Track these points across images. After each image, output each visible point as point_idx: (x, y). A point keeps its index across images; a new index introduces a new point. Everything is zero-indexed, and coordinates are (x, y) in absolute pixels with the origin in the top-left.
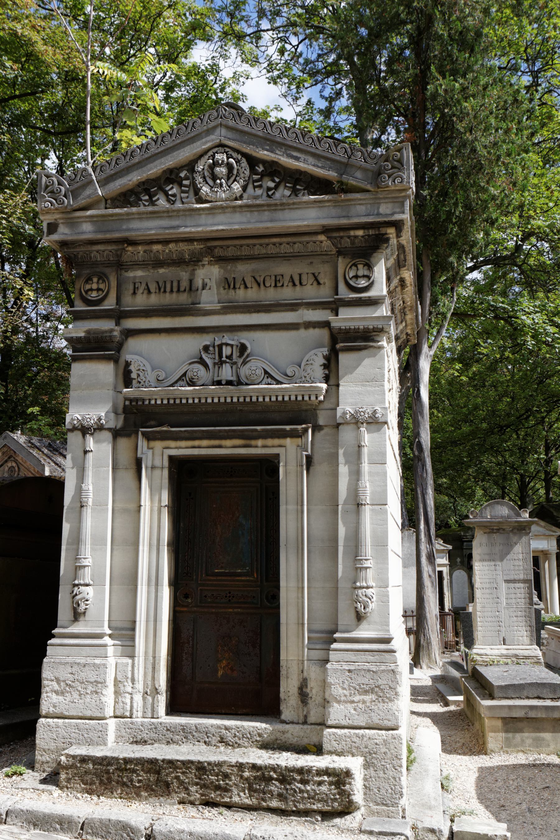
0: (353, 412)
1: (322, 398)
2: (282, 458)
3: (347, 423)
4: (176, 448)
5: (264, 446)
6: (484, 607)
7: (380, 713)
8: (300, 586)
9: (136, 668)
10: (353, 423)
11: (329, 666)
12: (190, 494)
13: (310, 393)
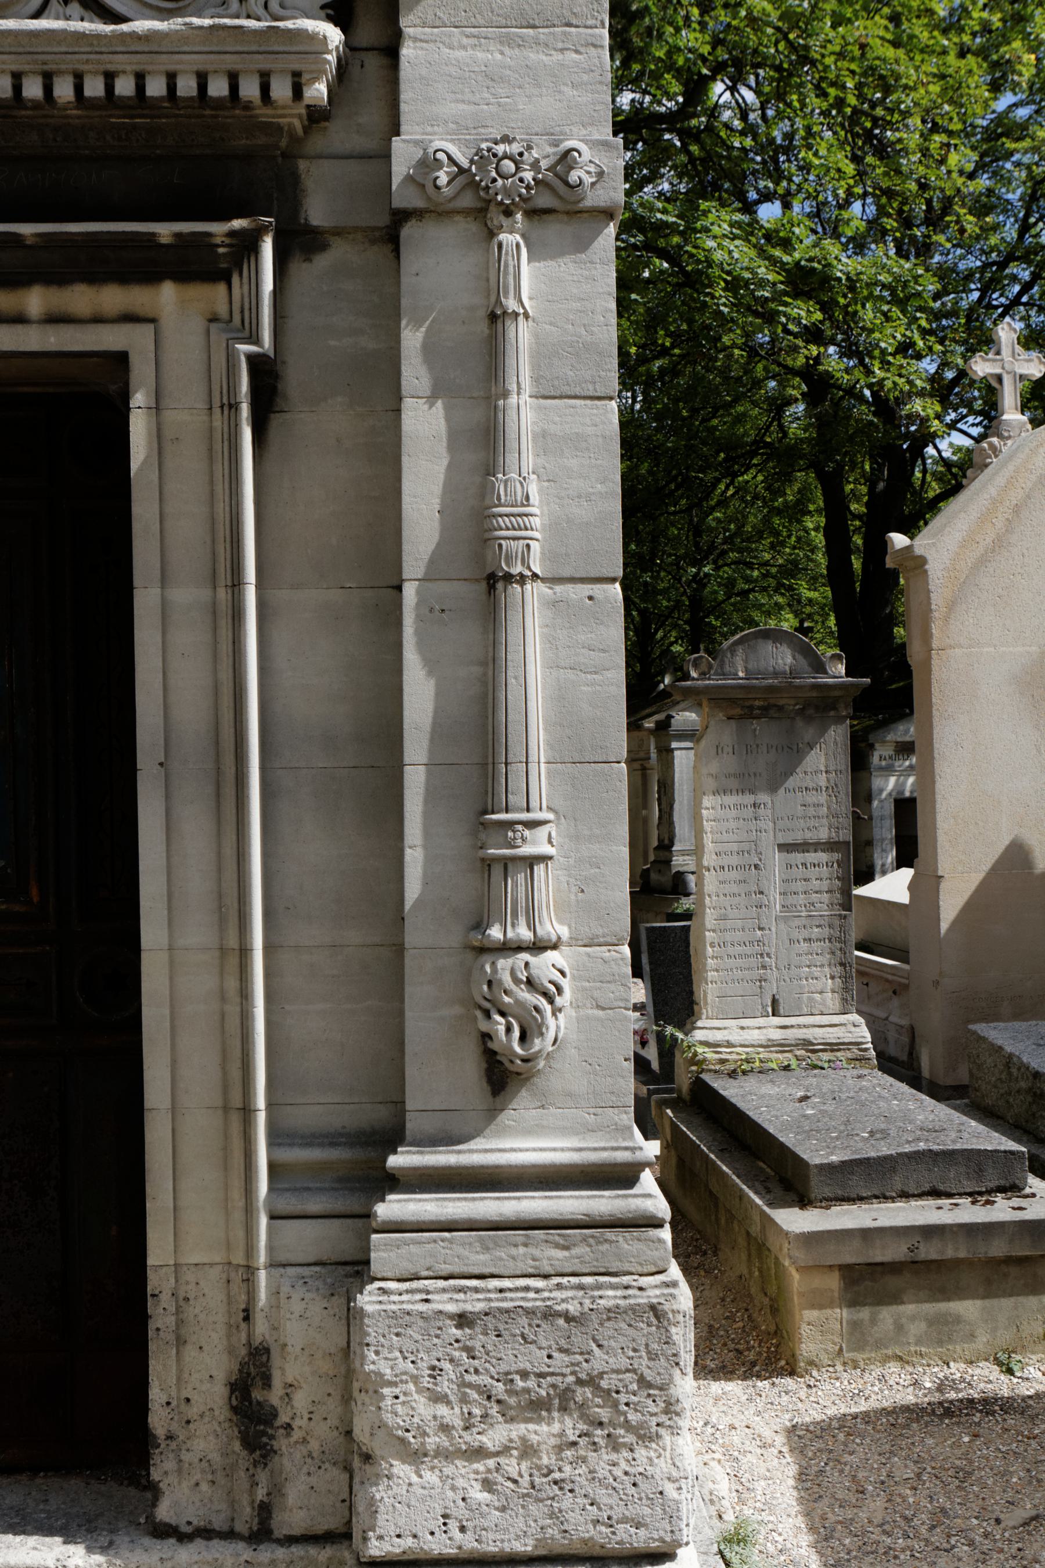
0: (465, 163)
1: (319, 90)
2: (141, 370)
3: (436, 212)
5: (55, 319)
6: (724, 918)
7: (602, 1495)
8: (233, 942)
10: (465, 212)
11: (368, 1300)
13: (263, 63)
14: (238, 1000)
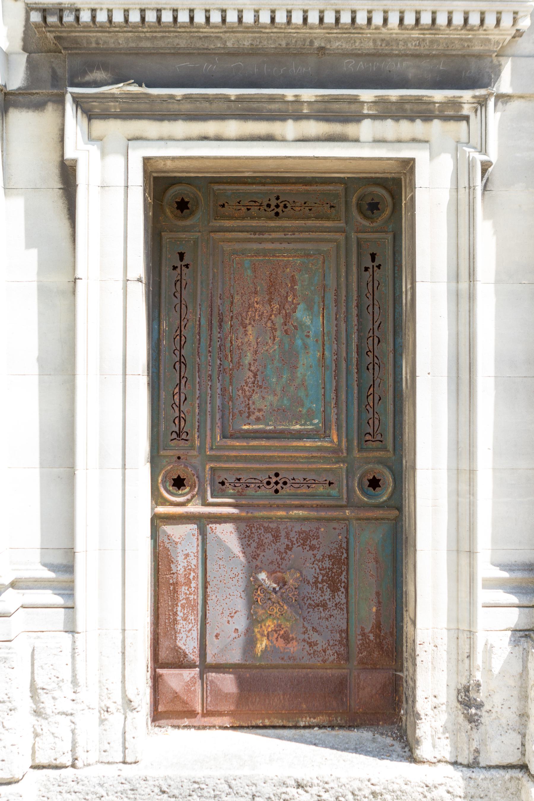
4: (161, 139)
5: (379, 141)
8: (464, 465)
9: (78, 659)
12: (181, 256)
14: (468, 496)
